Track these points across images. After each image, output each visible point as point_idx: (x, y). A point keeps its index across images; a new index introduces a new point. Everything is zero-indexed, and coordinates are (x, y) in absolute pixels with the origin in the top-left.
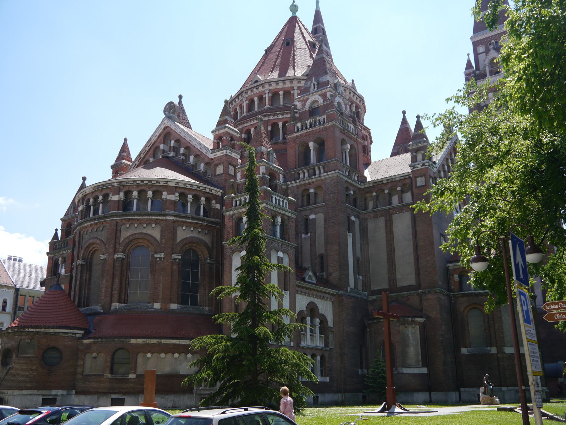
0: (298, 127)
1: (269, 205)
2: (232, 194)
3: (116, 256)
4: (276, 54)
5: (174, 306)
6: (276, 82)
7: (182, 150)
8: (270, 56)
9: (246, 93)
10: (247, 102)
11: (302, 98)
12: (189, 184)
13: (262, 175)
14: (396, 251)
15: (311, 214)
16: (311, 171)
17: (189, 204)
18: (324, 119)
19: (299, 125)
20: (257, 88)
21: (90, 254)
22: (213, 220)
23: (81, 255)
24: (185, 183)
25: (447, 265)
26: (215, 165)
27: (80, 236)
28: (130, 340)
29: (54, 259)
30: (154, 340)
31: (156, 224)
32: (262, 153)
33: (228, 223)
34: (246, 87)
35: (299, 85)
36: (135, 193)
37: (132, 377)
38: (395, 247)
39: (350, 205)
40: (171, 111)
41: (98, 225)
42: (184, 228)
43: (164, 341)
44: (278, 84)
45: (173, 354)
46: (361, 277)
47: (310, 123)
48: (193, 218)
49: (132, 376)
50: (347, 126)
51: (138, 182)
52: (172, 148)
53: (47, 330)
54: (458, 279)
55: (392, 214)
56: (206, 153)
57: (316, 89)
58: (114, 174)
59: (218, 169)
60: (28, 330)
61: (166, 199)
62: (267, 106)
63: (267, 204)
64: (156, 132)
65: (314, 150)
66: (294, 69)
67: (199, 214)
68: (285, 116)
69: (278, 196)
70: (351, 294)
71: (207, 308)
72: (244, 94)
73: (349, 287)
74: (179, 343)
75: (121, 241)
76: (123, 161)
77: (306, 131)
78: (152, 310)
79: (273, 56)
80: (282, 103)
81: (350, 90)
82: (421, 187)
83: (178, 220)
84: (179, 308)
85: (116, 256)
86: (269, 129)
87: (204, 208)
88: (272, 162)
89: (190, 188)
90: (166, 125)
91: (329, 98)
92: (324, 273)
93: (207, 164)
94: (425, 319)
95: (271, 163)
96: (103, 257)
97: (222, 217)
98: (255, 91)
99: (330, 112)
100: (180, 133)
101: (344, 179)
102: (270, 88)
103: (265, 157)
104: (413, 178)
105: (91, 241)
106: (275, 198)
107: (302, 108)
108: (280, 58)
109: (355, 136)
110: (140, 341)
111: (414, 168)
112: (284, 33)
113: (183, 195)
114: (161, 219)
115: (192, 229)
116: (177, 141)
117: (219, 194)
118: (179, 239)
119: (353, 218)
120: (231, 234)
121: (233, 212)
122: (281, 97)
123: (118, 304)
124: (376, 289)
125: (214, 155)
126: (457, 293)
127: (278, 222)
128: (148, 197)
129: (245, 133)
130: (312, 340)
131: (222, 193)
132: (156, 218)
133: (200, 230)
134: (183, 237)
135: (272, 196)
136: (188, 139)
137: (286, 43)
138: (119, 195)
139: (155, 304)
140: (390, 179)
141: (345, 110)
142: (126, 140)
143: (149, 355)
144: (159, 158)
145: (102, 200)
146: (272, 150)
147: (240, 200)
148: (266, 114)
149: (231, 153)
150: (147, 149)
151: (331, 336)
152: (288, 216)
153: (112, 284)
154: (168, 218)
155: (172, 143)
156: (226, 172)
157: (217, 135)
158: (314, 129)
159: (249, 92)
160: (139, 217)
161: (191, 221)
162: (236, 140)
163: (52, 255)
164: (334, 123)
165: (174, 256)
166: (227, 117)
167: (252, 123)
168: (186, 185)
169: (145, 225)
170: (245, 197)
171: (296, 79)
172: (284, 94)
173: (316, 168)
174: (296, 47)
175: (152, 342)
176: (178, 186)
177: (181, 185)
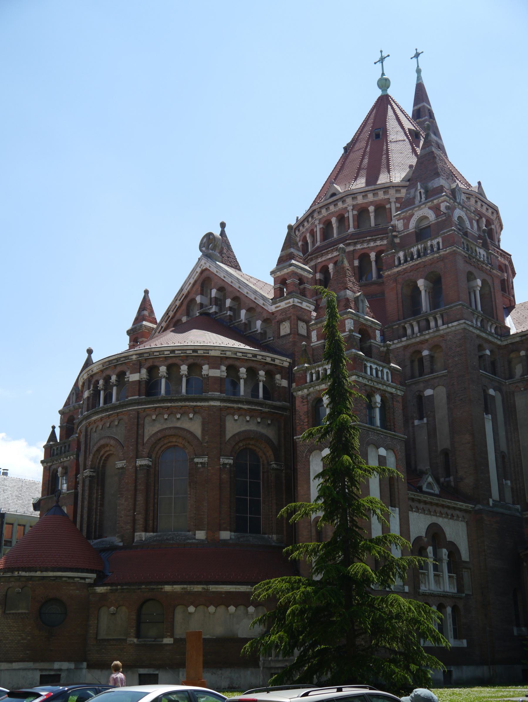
0: (399, 258)
1: (361, 378)
2: (304, 364)
3: (139, 462)
4: (361, 152)
5: (225, 535)
6: (363, 194)
7: (228, 302)
8: (352, 156)
9: (319, 212)
10: (321, 226)
11: (403, 214)
12: (240, 352)
13: (348, 333)
15: (426, 388)
16: (423, 324)
17: (242, 382)
18: (438, 243)
19: (401, 254)
20: (335, 203)
21: (102, 462)
22: (278, 403)
23: (89, 463)
24: (235, 351)
26: (278, 322)
27: (86, 435)
28: (163, 587)
29: (52, 469)
30: (199, 586)
31: (195, 413)
32: (347, 300)
33: (301, 408)
34: (318, 203)
35: (398, 195)
36: (163, 369)
37: (168, 642)
39: (486, 372)
40: (211, 246)
41: (112, 419)
42: (236, 417)
43: (213, 588)
44: (366, 195)
45: (227, 606)
46: (509, 482)
47: (418, 251)
48: (248, 403)
49: (168, 641)
50: (474, 251)
51: (166, 353)
52: (213, 300)
53: (45, 574)
56: (264, 304)
57: (423, 199)
58: (132, 343)
59: (282, 327)
60: (18, 573)
61: (207, 375)
62: (351, 230)
63: (359, 376)
64: (189, 277)
65: (426, 291)
66: (389, 172)
67: (258, 396)
68: (378, 243)
69: (375, 363)
70: (495, 509)
71: (275, 537)
72: (316, 215)
73: (491, 498)
74: (234, 590)
75: (145, 440)
76: (145, 323)
77: (412, 263)
78: (194, 541)
79: (356, 155)
80: (373, 224)
81: (476, 197)
83: (226, 406)
84: (233, 537)
85: (139, 462)
86: (356, 263)
87: (264, 387)
88: (363, 313)
89: (243, 357)
90: (204, 268)
91: (445, 211)
92: (452, 478)
93: (266, 321)
95: (362, 315)
96: (120, 464)
97: (292, 399)
98: (332, 208)
99: (447, 232)
100: (225, 277)
101: (474, 333)
102: (355, 203)
103: (352, 305)
105: (102, 442)
106: (371, 367)
107: (404, 230)
108: (366, 157)
109: (487, 266)
110: (178, 588)
112: (371, 121)
113: (232, 369)
114: (202, 406)
115: (248, 418)
116: (221, 289)
117: (286, 364)
118: (229, 435)
119: (491, 392)
120: (307, 423)
121: (308, 390)
122: (372, 216)
123: (143, 534)
125: (276, 307)
127: (376, 403)
128: (181, 374)
129: (320, 272)
130: (437, 582)
131: (290, 363)
132: (195, 404)
133: (259, 420)
134: (236, 432)
135: (365, 364)
136: (236, 286)
137: (374, 136)
138: (140, 373)
139: (197, 532)
141: (469, 227)
142: (146, 292)
143: (191, 609)
144: (195, 316)
145: (116, 381)
146: (362, 295)
147: (318, 372)
148: (350, 241)
149: (301, 303)
150: (178, 303)
151: (466, 575)
152: (391, 393)
153: (135, 505)
154: (212, 403)
155: (214, 292)
156: (294, 330)
157: (278, 277)
158: (424, 259)
159: (324, 211)
160: (169, 405)
161: (245, 407)
162: (307, 283)
163: (49, 464)
164: (455, 248)
165: (223, 460)
166: (292, 250)
167: (330, 256)
168: (236, 354)
169: (178, 416)
170: (324, 367)
171: (393, 187)
172: (376, 211)
173: (431, 319)
174: (390, 139)
175: (196, 590)
176: (224, 355)
177: (229, 354)
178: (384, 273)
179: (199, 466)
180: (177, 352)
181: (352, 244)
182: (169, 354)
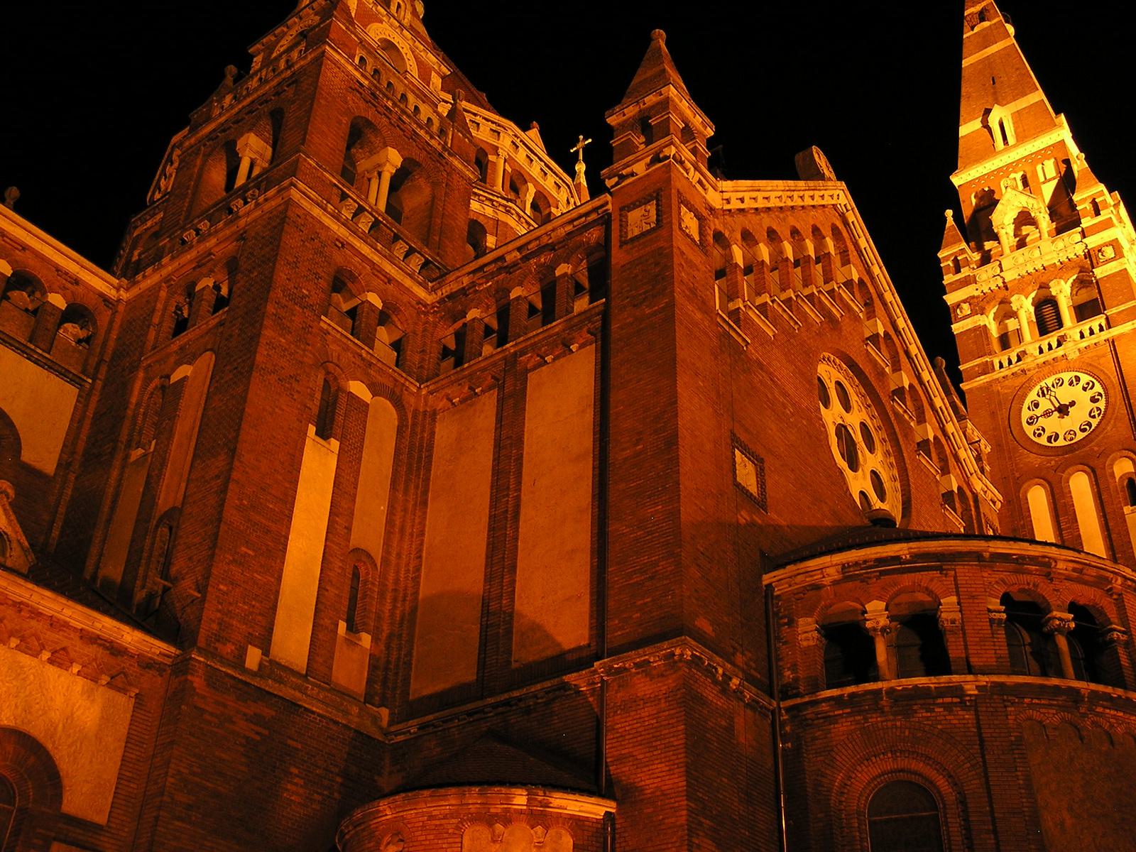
14: (526, 512)
25: (767, 579)
54: (816, 634)
55: (527, 371)
81: (516, 136)
82: (643, 234)
94: (610, 806)
104: (615, 216)
111: (622, 178)
124: (426, 692)
126: (807, 699)
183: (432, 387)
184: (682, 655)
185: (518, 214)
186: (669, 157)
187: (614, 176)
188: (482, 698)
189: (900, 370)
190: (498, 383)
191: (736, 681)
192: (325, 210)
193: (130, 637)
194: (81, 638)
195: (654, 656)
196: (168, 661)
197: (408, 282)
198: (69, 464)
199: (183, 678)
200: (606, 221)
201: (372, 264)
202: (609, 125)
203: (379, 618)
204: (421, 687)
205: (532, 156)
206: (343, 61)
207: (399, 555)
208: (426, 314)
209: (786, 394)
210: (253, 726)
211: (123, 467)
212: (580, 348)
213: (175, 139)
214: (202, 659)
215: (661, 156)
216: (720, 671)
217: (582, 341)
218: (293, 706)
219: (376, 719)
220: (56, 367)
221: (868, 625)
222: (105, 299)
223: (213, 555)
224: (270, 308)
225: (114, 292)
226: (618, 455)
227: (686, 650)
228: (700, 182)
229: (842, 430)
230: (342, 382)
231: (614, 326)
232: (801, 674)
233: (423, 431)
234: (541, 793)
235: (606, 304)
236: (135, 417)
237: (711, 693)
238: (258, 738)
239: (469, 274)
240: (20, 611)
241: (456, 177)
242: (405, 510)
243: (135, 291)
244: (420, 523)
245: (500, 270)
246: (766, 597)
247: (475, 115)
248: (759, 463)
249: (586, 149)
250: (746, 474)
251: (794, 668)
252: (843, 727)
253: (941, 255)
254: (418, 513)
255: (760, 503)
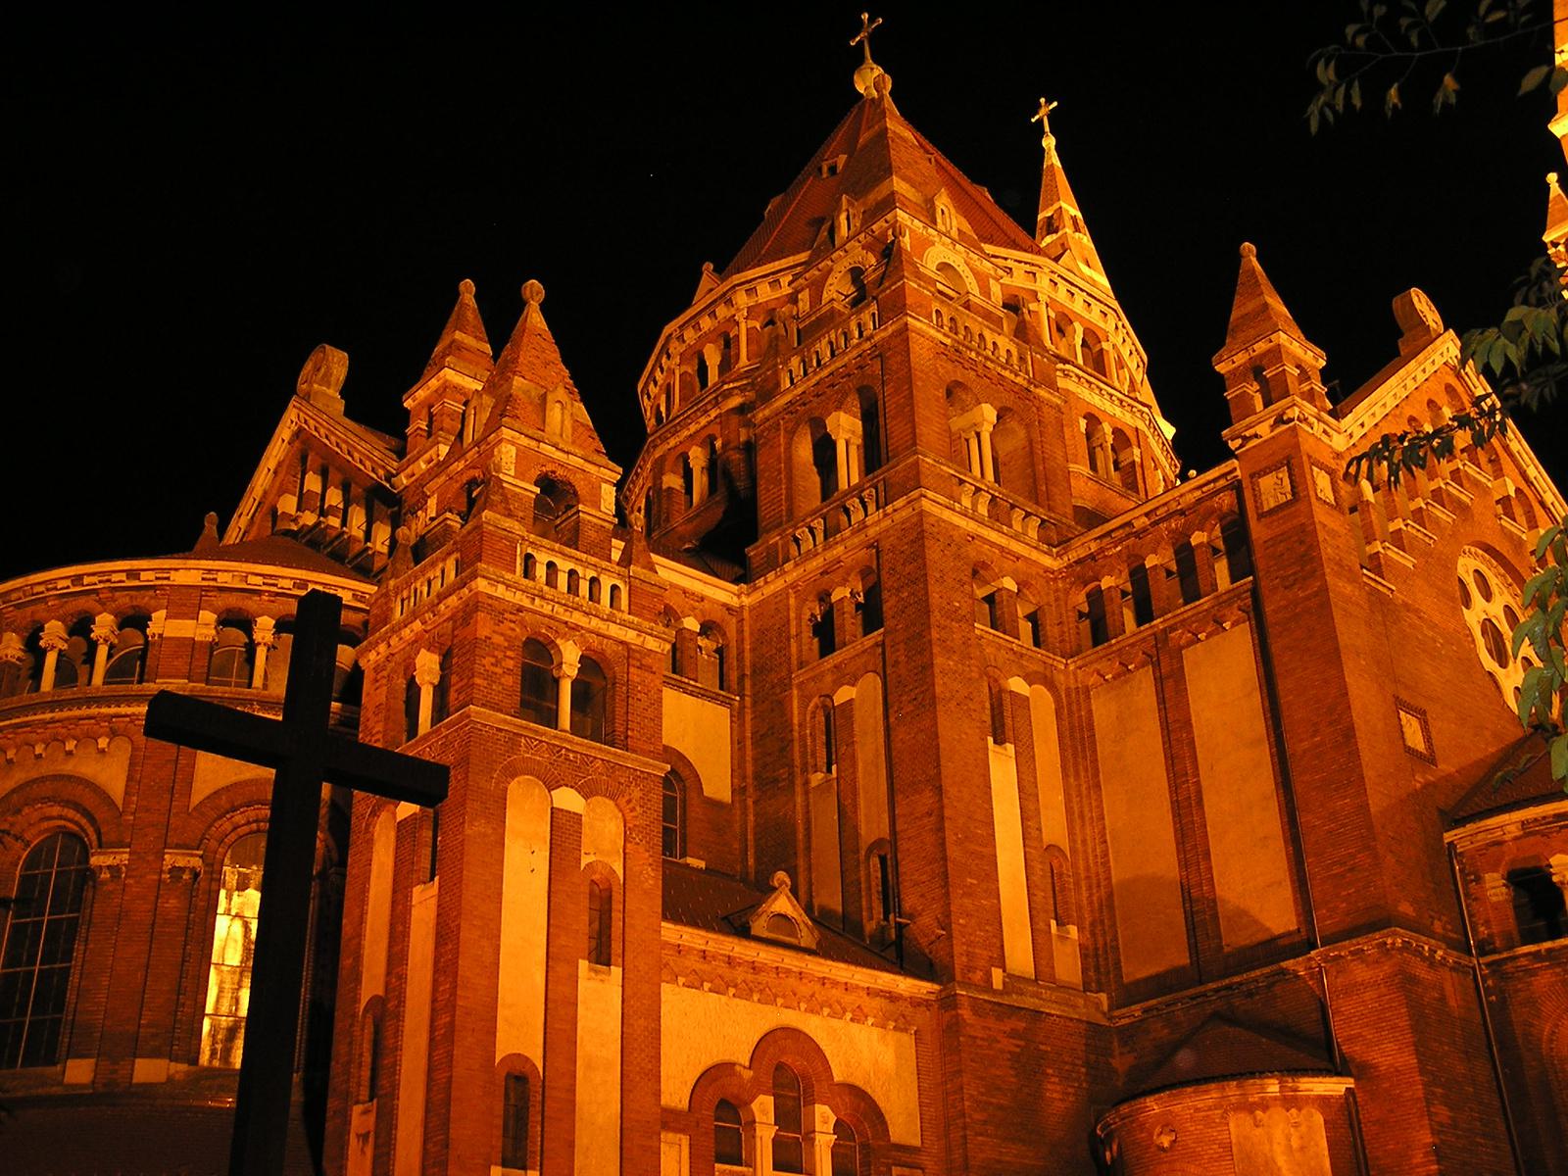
1: (501, 588)
6: (770, 279)
25: (1448, 837)
31: (113, 734)
38: (1204, 784)
54: (1504, 890)
55: (1181, 648)
61: (160, 636)
81: (1052, 272)
82: (1280, 507)
94: (1349, 1083)
98: (706, 323)
106: (551, 565)
111: (1246, 439)
113: (238, 620)
114: (134, 714)
118: (201, 791)
126: (1505, 955)
132: (113, 710)
140: (1157, 508)
141: (976, 292)
148: (731, 385)
160: (48, 716)
176: (212, 583)
178: (754, 416)
179: (102, 876)
180: (86, 580)
181: (736, 391)
182: (68, 587)
183: (1079, 663)
184: (1393, 944)
185: (1077, 375)
186: (1293, 420)
187: (1237, 438)
188: (1201, 983)
189: (1537, 527)
190: (1153, 660)
191: (1440, 953)
192: (954, 510)
193: (905, 985)
194: (868, 994)
195: (1368, 944)
196: (932, 997)
197: (1035, 555)
198: (744, 789)
199: (954, 1012)
200: (1237, 487)
201: (1002, 549)
202: (1218, 373)
203: (1080, 908)
204: (1136, 970)
205: (1074, 290)
206: (924, 327)
207: (1084, 842)
208: (1055, 580)
209: (1433, 627)
210: (1015, 1042)
211: (806, 793)
212: (1233, 625)
213: (667, 330)
214: (964, 993)
215: (1285, 418)
216: (1426, 948)
217: (1234, 618)
218: (1037, 1013)
219: (1098, 1005)
220: (708, 694)
221: (1555, 879)
222: (728, 608)
223: (947, 893)
224: (935, 635)
225: (735, 598)
226: (1297, 746)
227: (1396, 939)
228: (1325, 432)
229: (1488, 628)
230: (1001, 682)
231: (1269, 609)
232: (1495, 929)
233: (1079, 710)
234: (1290, 1080)
235: (1255, 582)
236: (803, 738)
237: (1421, 971)
238: (1018, 1050)
239: (1096, 539)
240: (824, 984)
241: (1045, 409)
242: (1079, 795)
243: (756, 597)
244: (1097, 807)
245: (1128, 537)
246: (1450, 855)
247: (1006, 259)
248: (1421, 714)
249: (1052, 115)
250: (1414, 737)
251: (1487, 923)
252: (1544, 980)
253: (1547, 238)
254: (1094, 797)
255: (1429, 759)
